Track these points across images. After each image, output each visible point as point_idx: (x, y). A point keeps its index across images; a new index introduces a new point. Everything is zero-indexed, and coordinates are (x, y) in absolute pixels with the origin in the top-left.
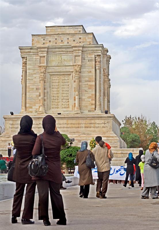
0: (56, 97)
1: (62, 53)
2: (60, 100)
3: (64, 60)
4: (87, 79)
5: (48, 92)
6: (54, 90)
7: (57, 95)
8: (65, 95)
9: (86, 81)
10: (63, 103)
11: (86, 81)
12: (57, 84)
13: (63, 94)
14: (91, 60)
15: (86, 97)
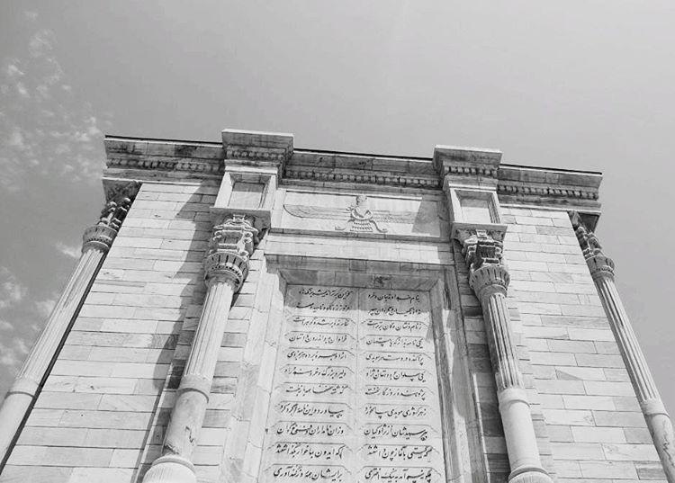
0: (318, 417)
1: (375, 186)
2: (355, 438)
3: (388, 217)
4: (556, 309)
5: (251, 372)
6: (302, 361)
7: (325, 397)
8: (398, 403)
9: (549, 319)
10: (376, 460)
11: (549, 319)
12: (335, 329)
13: (378, 399)
14: (555, 229)
15: (579, 416)
